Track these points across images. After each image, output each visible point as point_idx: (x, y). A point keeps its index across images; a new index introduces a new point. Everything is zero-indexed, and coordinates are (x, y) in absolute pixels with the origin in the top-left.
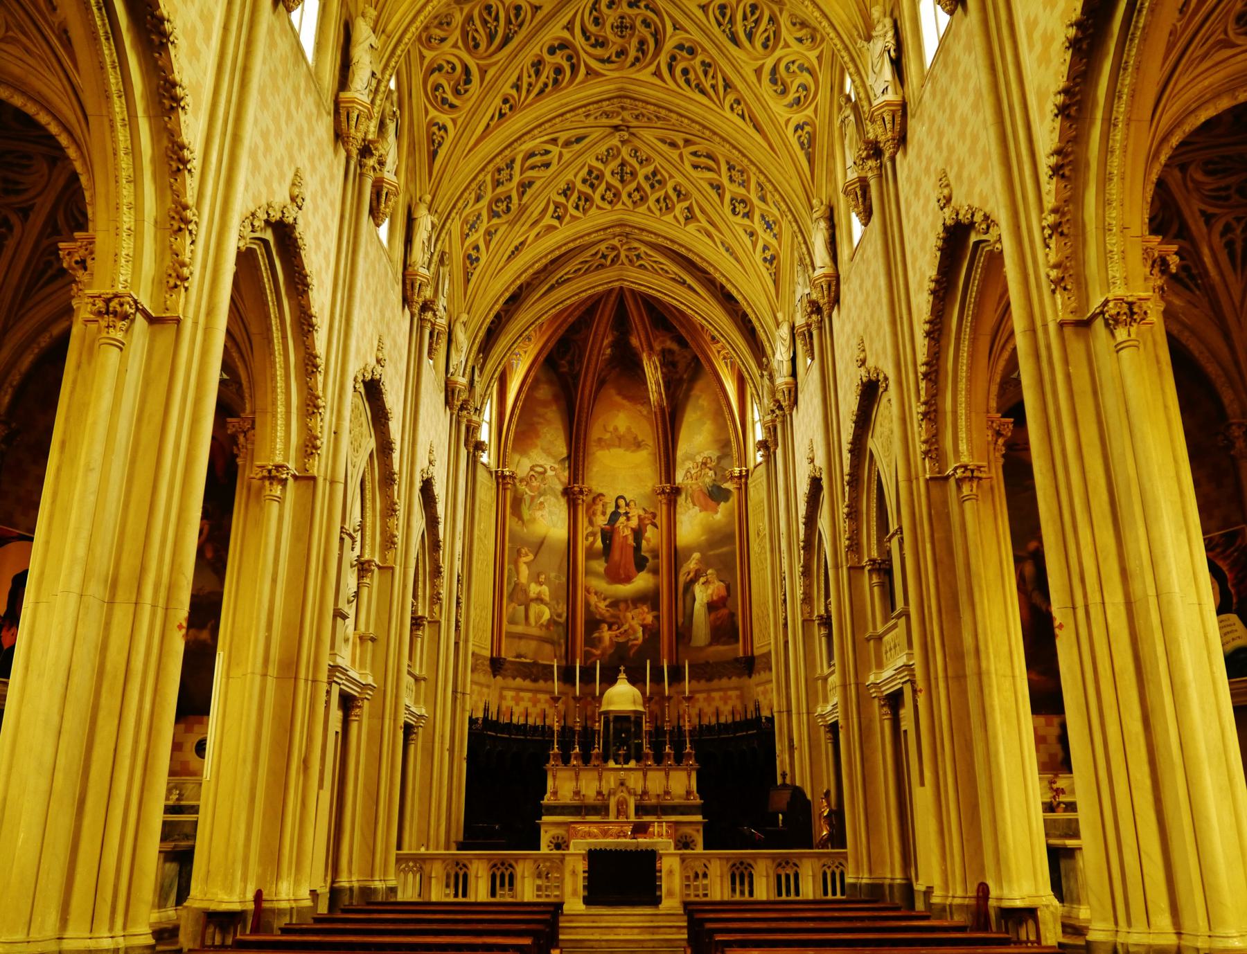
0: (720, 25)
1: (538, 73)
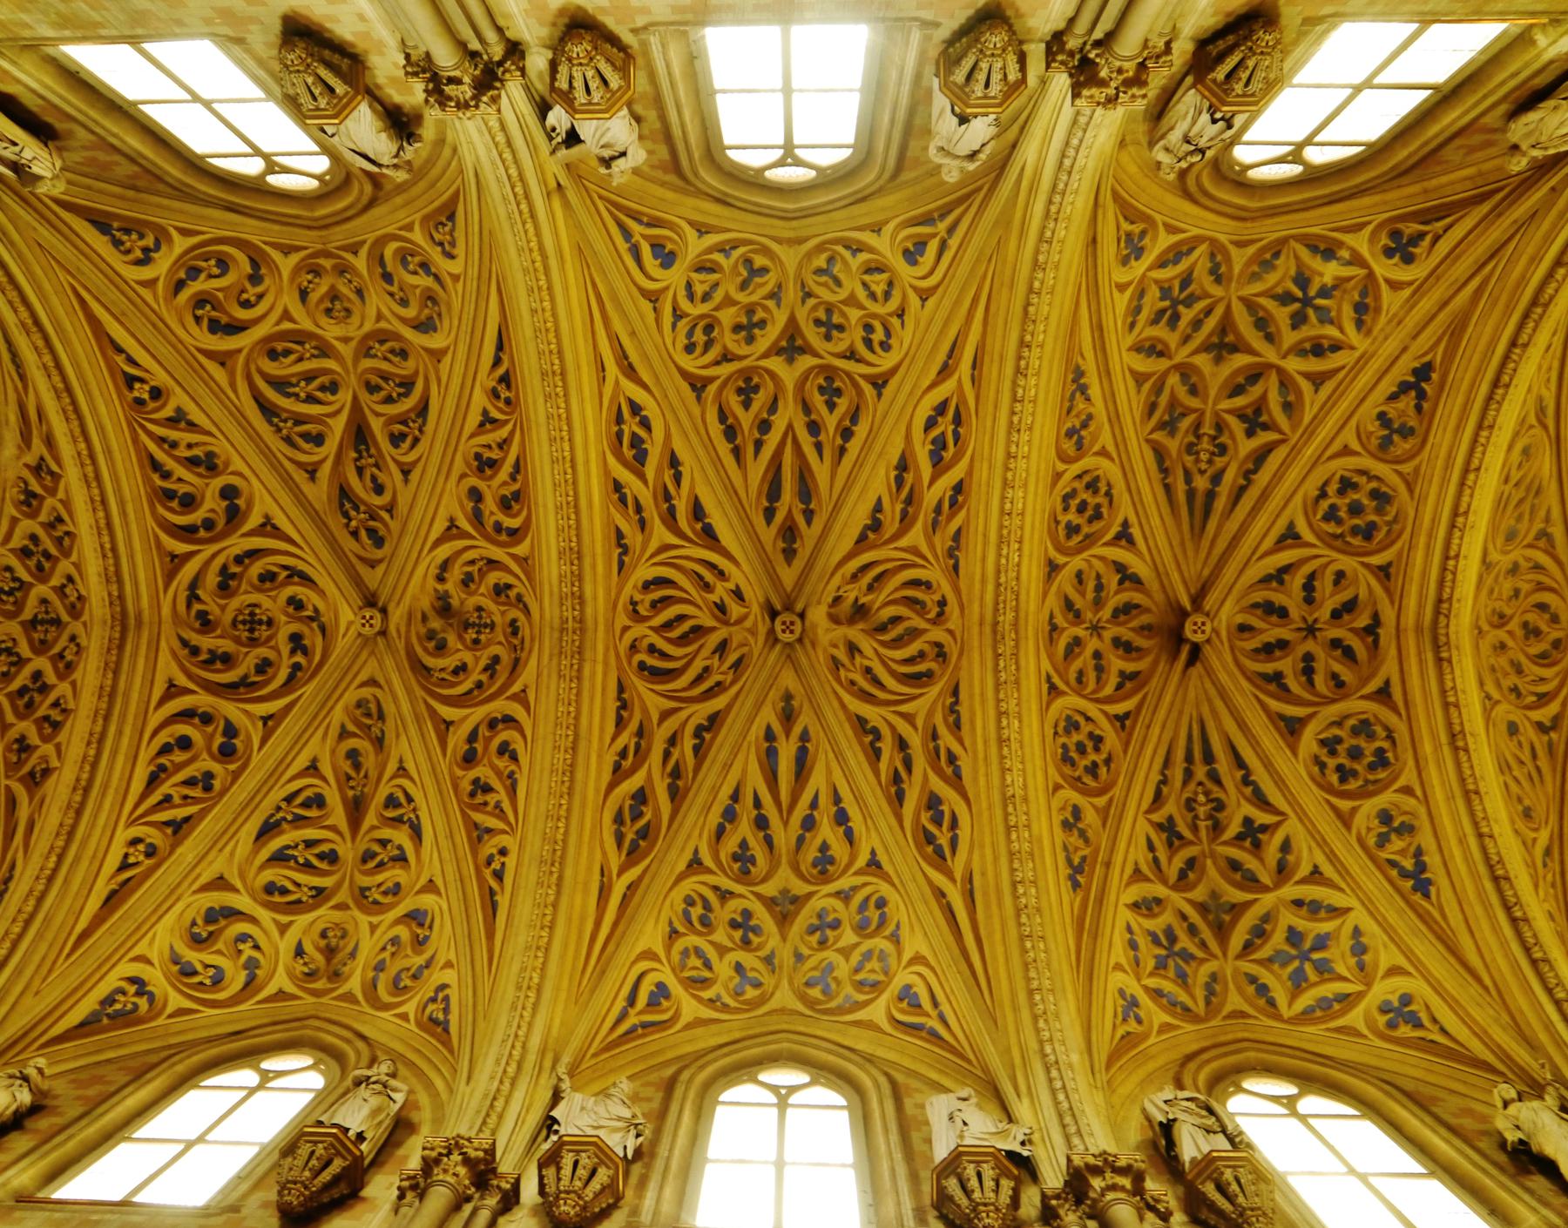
0: (289, 799)
1: (193, 462)
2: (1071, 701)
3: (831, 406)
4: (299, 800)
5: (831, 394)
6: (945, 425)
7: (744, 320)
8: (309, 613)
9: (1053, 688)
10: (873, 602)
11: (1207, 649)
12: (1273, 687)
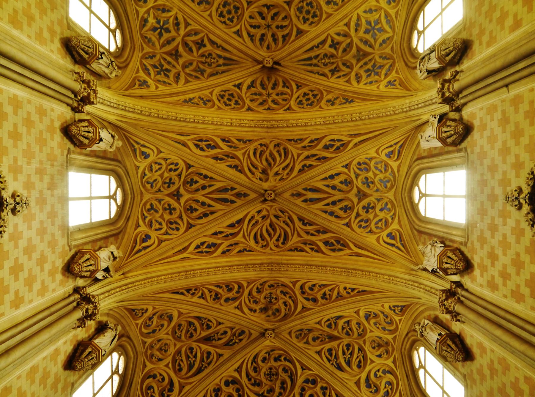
0: (329, 361)
2: (293, 103)
3: (197, 182)
4: (329, 357)
5: (192, 182)
6: (203, 145)
7: (168, 211)
8: (267, 355)
9: (288, 109)
10: (261, 167)
11: (275, 59)
12: (287, 38)
